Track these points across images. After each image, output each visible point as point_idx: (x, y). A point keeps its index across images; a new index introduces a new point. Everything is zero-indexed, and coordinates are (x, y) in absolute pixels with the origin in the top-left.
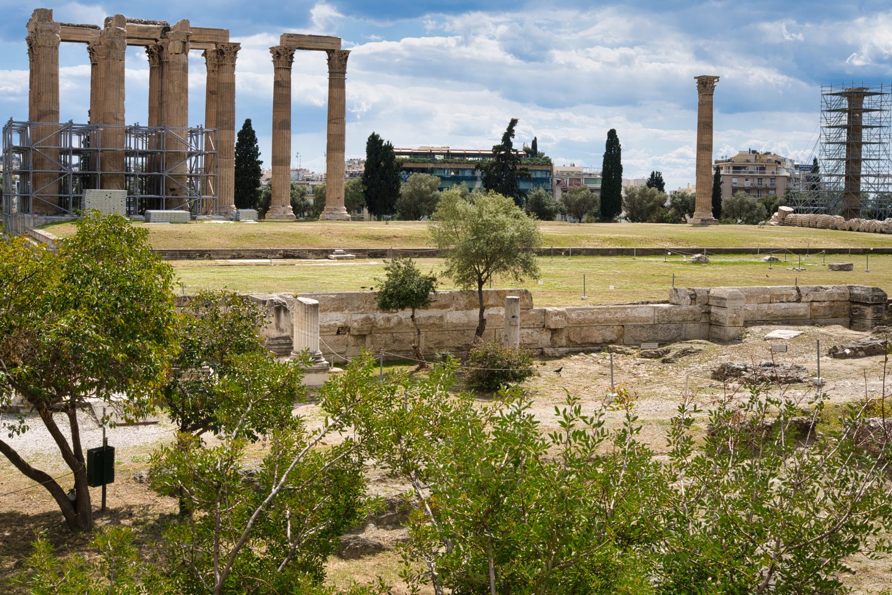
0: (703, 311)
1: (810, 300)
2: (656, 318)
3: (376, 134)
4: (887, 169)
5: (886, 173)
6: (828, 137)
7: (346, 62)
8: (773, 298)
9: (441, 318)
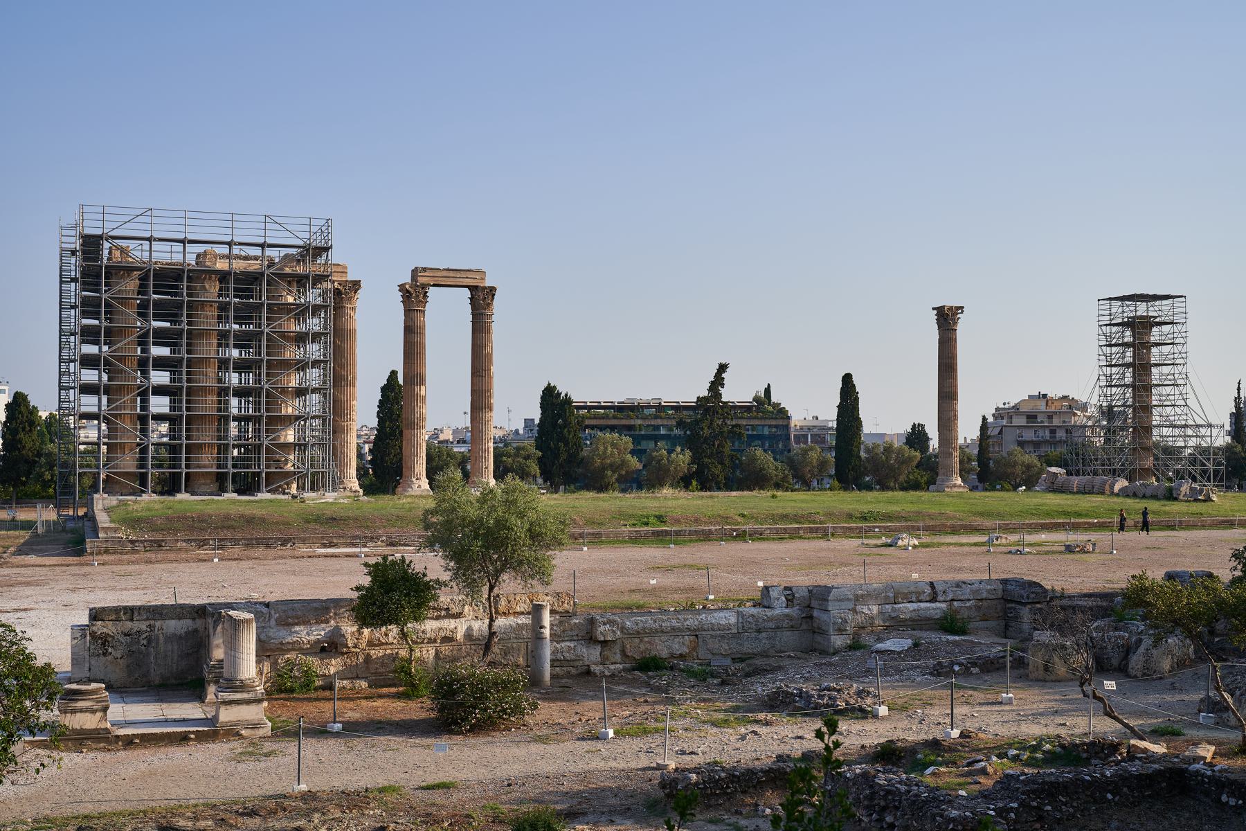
1: (948, 599)
3: (552, 385)
4: (1185, 418)
5: (1183, 423)
6: (1109, 378)
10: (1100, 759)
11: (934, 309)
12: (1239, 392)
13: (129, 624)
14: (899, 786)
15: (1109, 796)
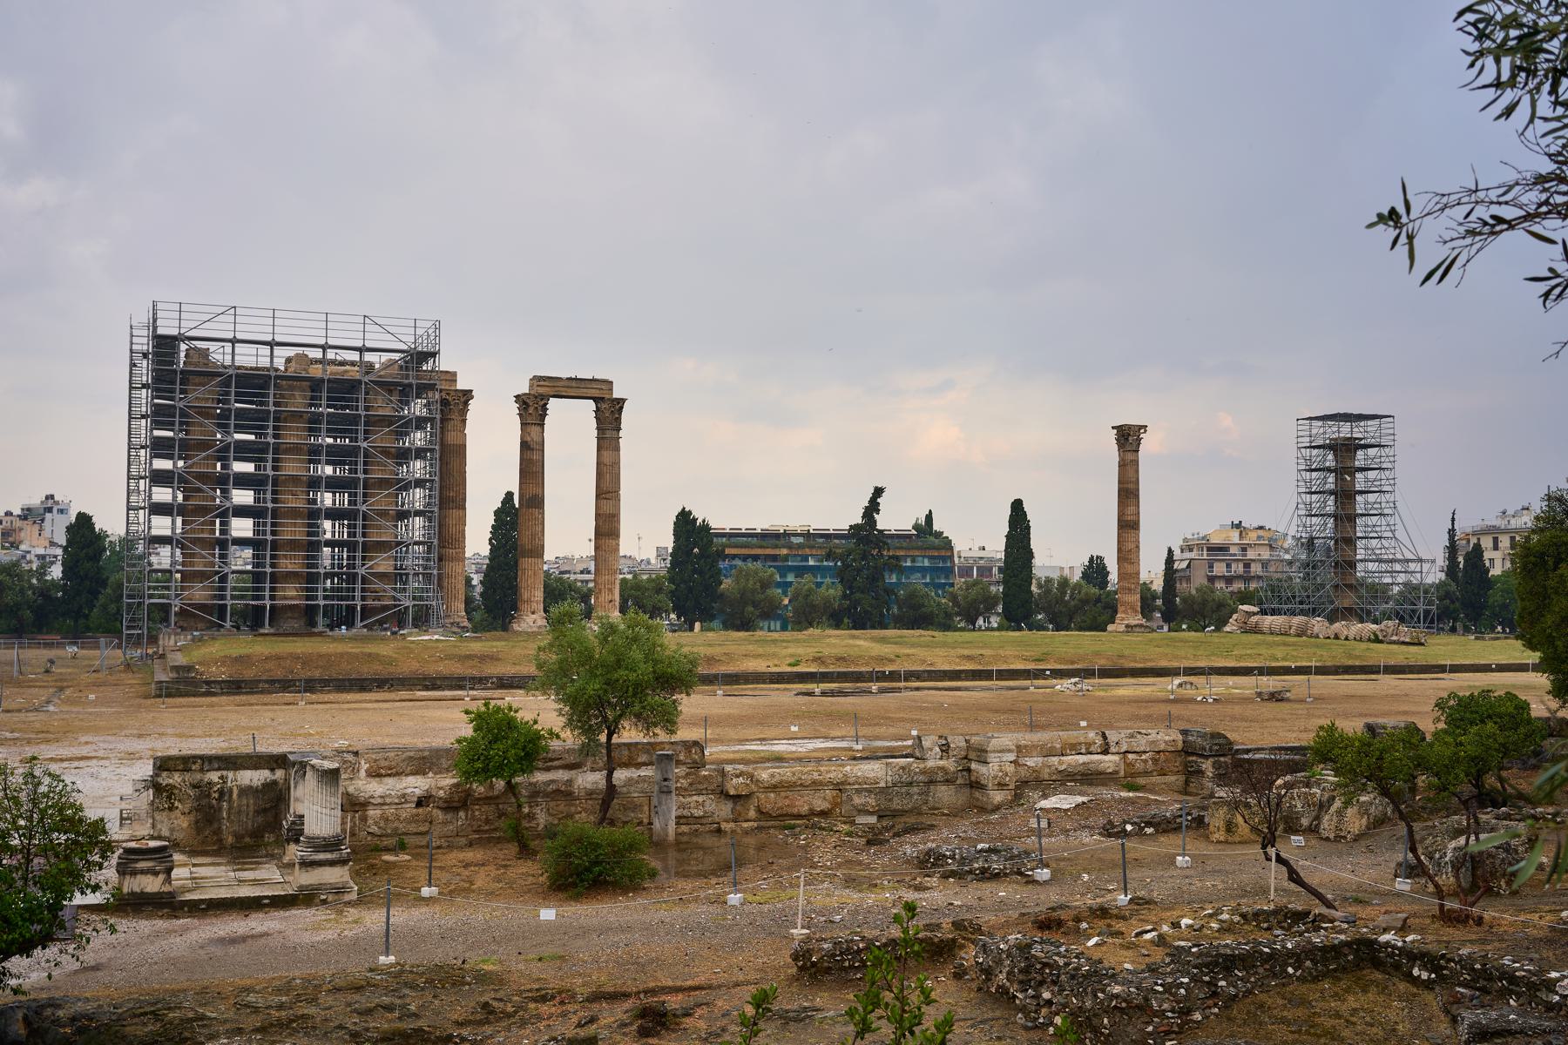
0: (960, 768)
1: (1122, 751)
2: (889, 779)
3: (687, 509)
4: (1393, 551)
5: (1391, 557)
7: (620, 414)
8: (1065, 749)
9: (570, 782)
10: (1282, 928)
11: (1113, 428)
12: (1453, 524)
13: (198, 776)
14: (1057, 958)
15: (1290, 970)
